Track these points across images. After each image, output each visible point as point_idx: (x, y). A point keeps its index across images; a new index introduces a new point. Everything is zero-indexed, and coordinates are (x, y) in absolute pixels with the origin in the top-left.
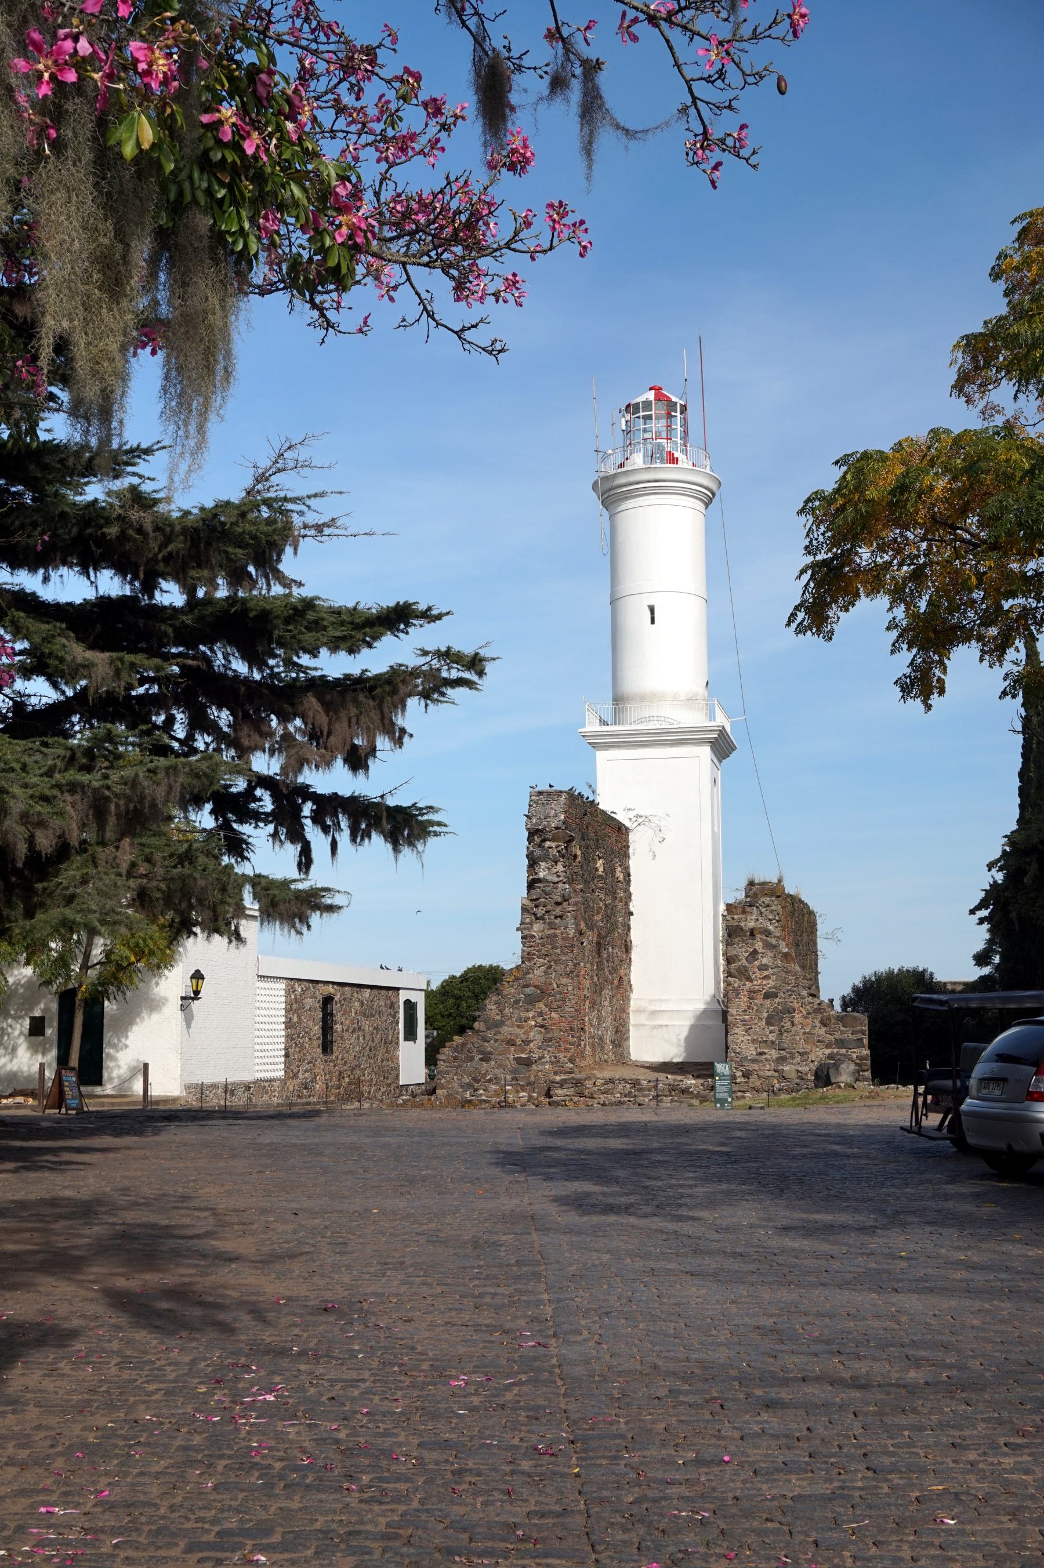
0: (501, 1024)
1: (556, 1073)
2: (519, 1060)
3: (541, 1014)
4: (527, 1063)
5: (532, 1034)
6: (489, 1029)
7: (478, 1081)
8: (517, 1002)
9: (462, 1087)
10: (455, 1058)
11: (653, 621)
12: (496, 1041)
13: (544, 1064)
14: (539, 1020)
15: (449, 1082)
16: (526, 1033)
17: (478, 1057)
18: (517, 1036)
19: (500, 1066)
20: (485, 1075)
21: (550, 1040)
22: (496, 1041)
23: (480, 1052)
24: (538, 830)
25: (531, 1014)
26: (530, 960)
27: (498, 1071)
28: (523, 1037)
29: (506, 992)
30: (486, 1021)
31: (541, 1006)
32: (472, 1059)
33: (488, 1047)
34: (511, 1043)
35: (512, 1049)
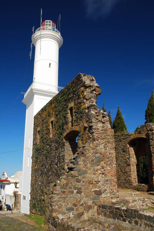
0: (85, 172)
1: (112, 198)
2: (95, 191)
3: (103, 168)
4: (99, 193)
5: (100, 178)
6: (79, 175)
7: (75, 205)
8: (92, 161)
9: (67, 210)
10: (64, 192)
11: (50, 67)
12: (83, 182)
13: (107, 193)
14: (103, 170)
15: (60, 207)
16: (98, 177)
17: (75, 191)
18: (93, 178)
19: (87, 196)
20: (80, 201)
21: (107, 180)
22: (83, 182)
23: (75, 188)
24: (90, 86)
25: (99, 167)
26: (98, 140)
27: (85, 199)
28: (96, 179)
29: (88, 155)
30: (79, 171)
31: (102, 163)
32: (73, 192)
33: (79, 185)
34: (90, 183)
35: (91, 186)
